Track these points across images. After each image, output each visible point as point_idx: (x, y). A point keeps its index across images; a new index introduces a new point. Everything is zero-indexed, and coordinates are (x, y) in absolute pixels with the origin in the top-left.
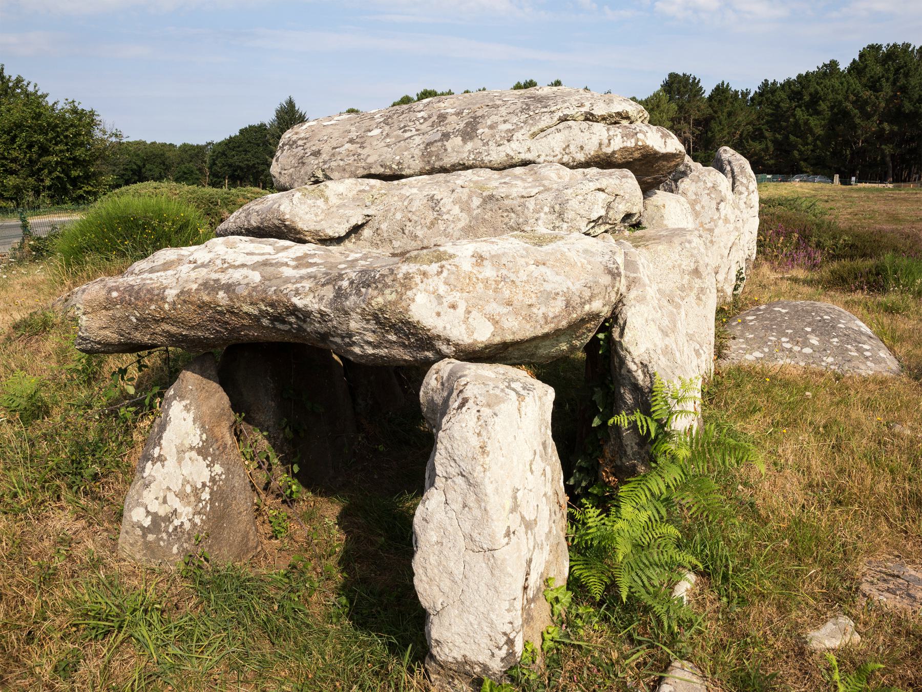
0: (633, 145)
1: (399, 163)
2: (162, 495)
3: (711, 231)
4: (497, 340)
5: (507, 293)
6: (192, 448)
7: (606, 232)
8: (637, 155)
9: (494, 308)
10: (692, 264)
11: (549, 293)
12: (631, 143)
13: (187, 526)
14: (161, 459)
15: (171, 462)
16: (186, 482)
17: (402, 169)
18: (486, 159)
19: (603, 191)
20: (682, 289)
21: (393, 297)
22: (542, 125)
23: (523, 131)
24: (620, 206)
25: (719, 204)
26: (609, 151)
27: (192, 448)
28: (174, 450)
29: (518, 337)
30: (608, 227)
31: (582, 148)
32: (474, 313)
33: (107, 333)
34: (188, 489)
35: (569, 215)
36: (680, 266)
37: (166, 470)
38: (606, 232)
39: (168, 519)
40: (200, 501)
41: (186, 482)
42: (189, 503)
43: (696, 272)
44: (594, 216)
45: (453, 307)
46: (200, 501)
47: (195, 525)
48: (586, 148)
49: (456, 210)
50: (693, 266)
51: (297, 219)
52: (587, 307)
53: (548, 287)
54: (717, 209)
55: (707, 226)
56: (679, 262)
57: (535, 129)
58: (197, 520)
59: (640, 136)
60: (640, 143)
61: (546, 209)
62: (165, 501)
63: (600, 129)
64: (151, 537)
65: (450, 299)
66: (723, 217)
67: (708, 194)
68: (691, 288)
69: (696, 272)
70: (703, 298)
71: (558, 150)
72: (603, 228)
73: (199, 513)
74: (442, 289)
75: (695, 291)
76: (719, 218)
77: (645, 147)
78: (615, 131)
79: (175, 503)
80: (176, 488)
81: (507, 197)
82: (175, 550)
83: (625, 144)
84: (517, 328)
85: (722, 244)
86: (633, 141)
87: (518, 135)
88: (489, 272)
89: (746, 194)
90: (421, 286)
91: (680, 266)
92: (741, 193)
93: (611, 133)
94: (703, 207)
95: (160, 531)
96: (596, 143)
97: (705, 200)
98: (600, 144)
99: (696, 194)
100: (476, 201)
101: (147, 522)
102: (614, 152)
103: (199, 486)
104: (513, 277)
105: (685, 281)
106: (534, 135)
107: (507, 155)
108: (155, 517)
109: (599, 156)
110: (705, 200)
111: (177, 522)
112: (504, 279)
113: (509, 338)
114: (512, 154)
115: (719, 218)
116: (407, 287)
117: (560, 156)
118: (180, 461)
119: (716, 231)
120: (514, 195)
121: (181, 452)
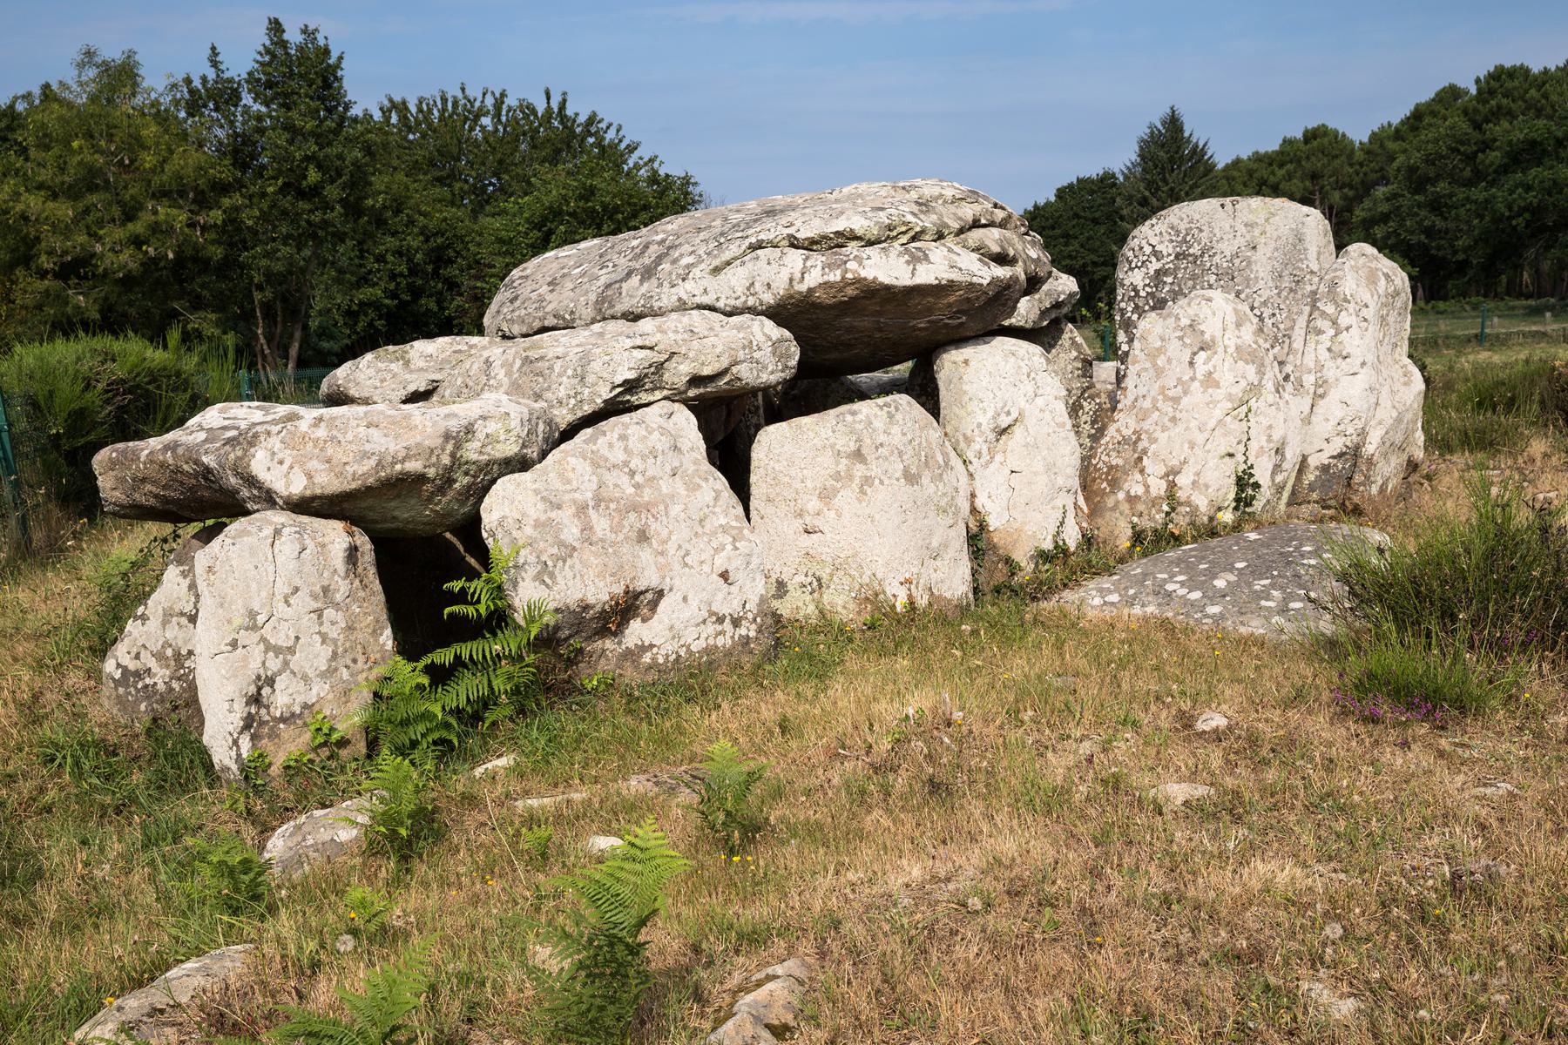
0: (838, 278)
1: (572, 313)
2: (135, 650)
3: (1176, 400)
4: (308, 493)
5: (330, 452)
6: (182, 614)
7: (665, 398)
8: (850, 291)
9: (314, 464)
10: (852, 444)
11: (365, 453)
12: (835, 276)
13: (161, 687)
14: (144, 618)
15: (153, 624)
16: (167, 644)
17: (573, 320)
18: (656, 305)
19: (651, 348)
20: (837, 477)
21: (239, 453)
22: (727, 256)
23: (702, 266)
24: (681, 367)
25: (1195, 354)
26: (803, 288)
27: (182, 614)
28: (160, 611)
29: (329, 491)
30: (665, 393)
31: (769, 285)
32: (296, 469)
33: (117, 493)
34: (169, 652)
35: (590, 379)
36: (833, 446)
37: (145, 628)
38: (665, 398)
39: (137, 675)
40: (183, 667)
41: (167, 644)
42: (168, 666)
43: (858, 455)
44: (619, 380)
45: (281, 463)
46: (183, 667)
47: (172, 689)
48: (773, 285)
49: (502, 373)
50: (853, 446)
51: (351, 385)
52: (398, 467)
53: (368, 447)
54: (1191, 363)
55: (1170, 393)
56: (832, 440)
57: (716, 262)
58: (175, 685)
59: (852, 265)
60: (849, 275)
61: (570, 372)
62: (137, 657)
63: (795, 258)
64: (121, 690)
65: (280, 456)
66: (1199, 376)
67: (1181, 338)
68: (851, 477)
69: (858, 455)
70: (869, 491)
71: (740, 290)
72: (658, 395)
73: (179, 679)
74: (278, 446)
75: (857, 481)
76: (1193, 379)
77: (858, 281)
78: (818, 259)
79: (152, 663)
80: (155, 646)
81: (542, 358)
82: (143, 707)
83: (826, 278)
84: (328, 483)
85: (1194, 424)
86: (838, 272)
87: (696, 272)
88: (321, 432)
89: (1332, 332)
90: (264, 444)
91: (833, 446)
92: (1320, 332)
93: (808, 264)
94: (1169, 361)
95: (127, 686)
96: (786, 279)
97: (1174, 347)
98: (791, 280)
99: (1163, 339)
100: (518, 363)
101: (118, 675)
102: (810, 290)
103: (184, 652)
104: (340, 437)
105: (842, 467)
106: (716, 270)
107: (680, 299)
108: (125, 670)
109: (791, 297)
110: (1174, 347)
111: (148, 681)
112: (333, 438)
113: (318, 491)
114: (685, 297)
115: (1193, 379)
116: (252, 444)
117: (743, 298)
118: (164, 624)
119: (1185, 401)
120: (550, 355)
121: (168, 616)
